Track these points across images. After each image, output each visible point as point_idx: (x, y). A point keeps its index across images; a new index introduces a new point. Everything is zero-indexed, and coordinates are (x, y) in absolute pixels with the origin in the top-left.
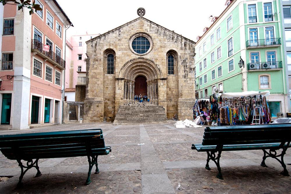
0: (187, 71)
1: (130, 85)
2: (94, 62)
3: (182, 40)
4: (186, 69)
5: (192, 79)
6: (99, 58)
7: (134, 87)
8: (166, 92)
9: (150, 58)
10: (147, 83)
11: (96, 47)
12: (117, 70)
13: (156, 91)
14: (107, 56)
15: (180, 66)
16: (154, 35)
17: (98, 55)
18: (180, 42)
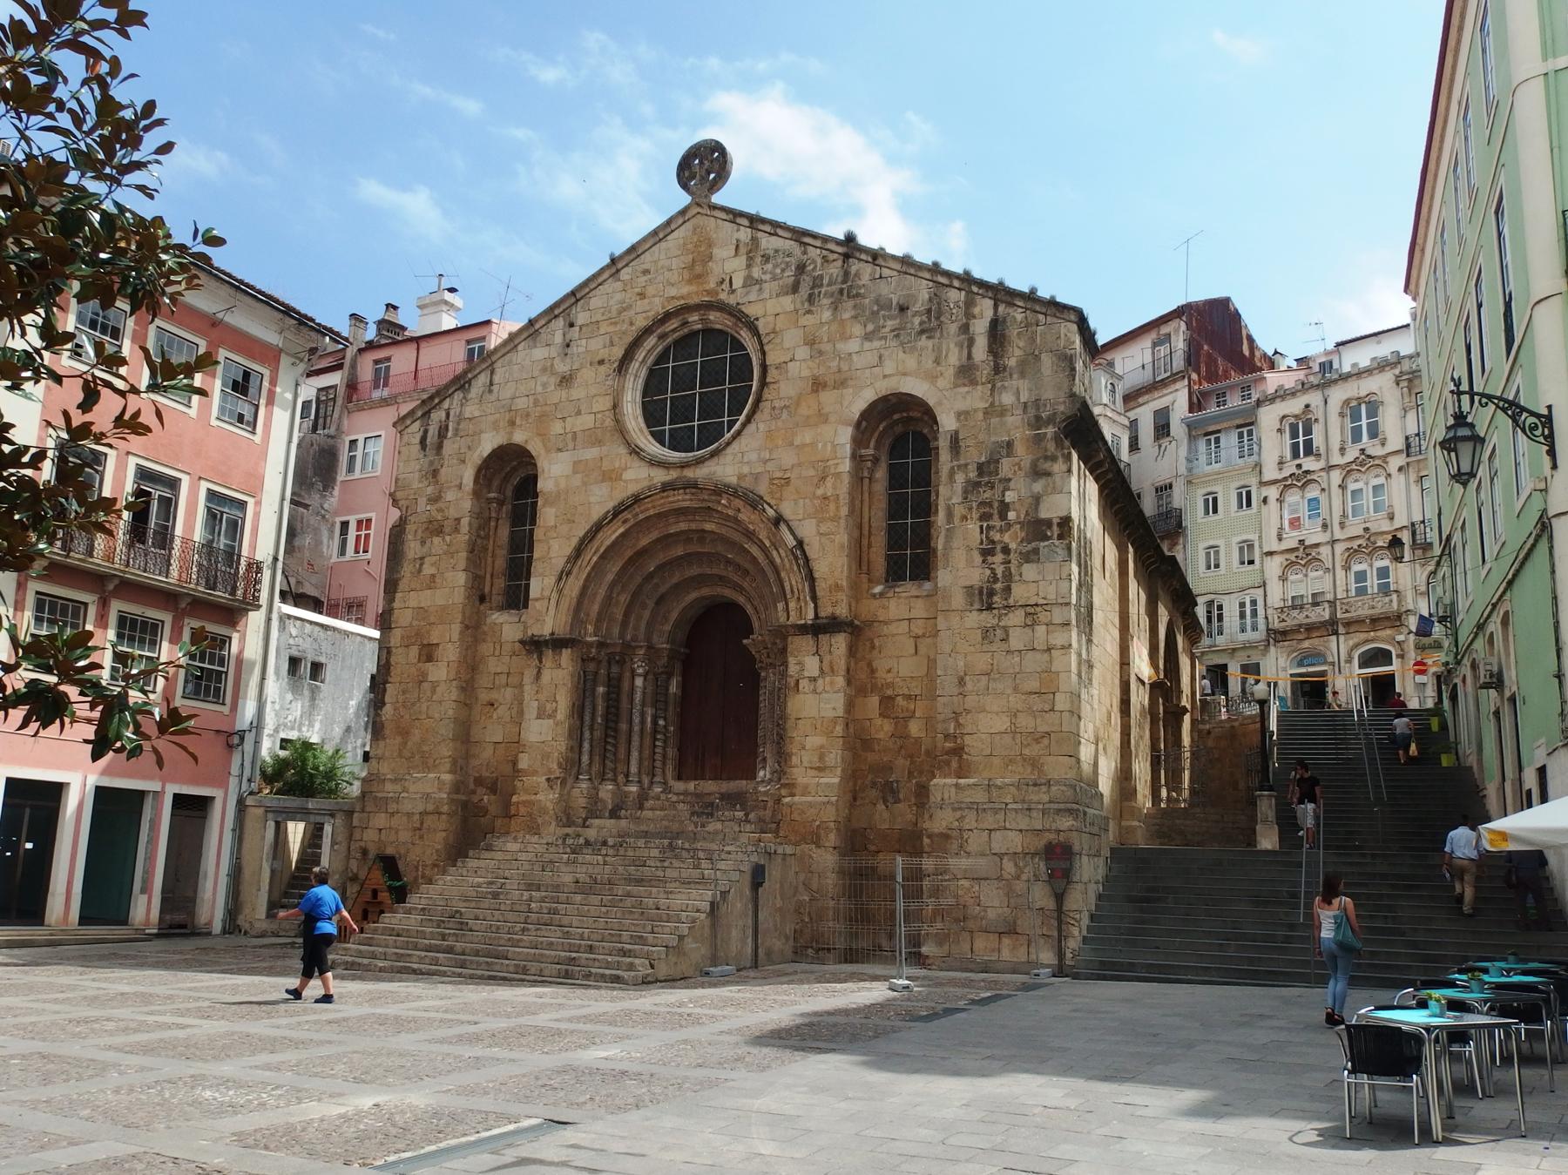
0: (1006, 550)
1: (639, 682)
2: (423, 543)
3: (976, 310)
4: (997, 537)
6: (452, 513)
7: (673, 688)
8: (839, 730)
9: (741, 477)
11: (439, 447)
12: (538, 585)
14: (509, 493)
16: (773, 306)
17: (450, 496)
18: (953, 328)
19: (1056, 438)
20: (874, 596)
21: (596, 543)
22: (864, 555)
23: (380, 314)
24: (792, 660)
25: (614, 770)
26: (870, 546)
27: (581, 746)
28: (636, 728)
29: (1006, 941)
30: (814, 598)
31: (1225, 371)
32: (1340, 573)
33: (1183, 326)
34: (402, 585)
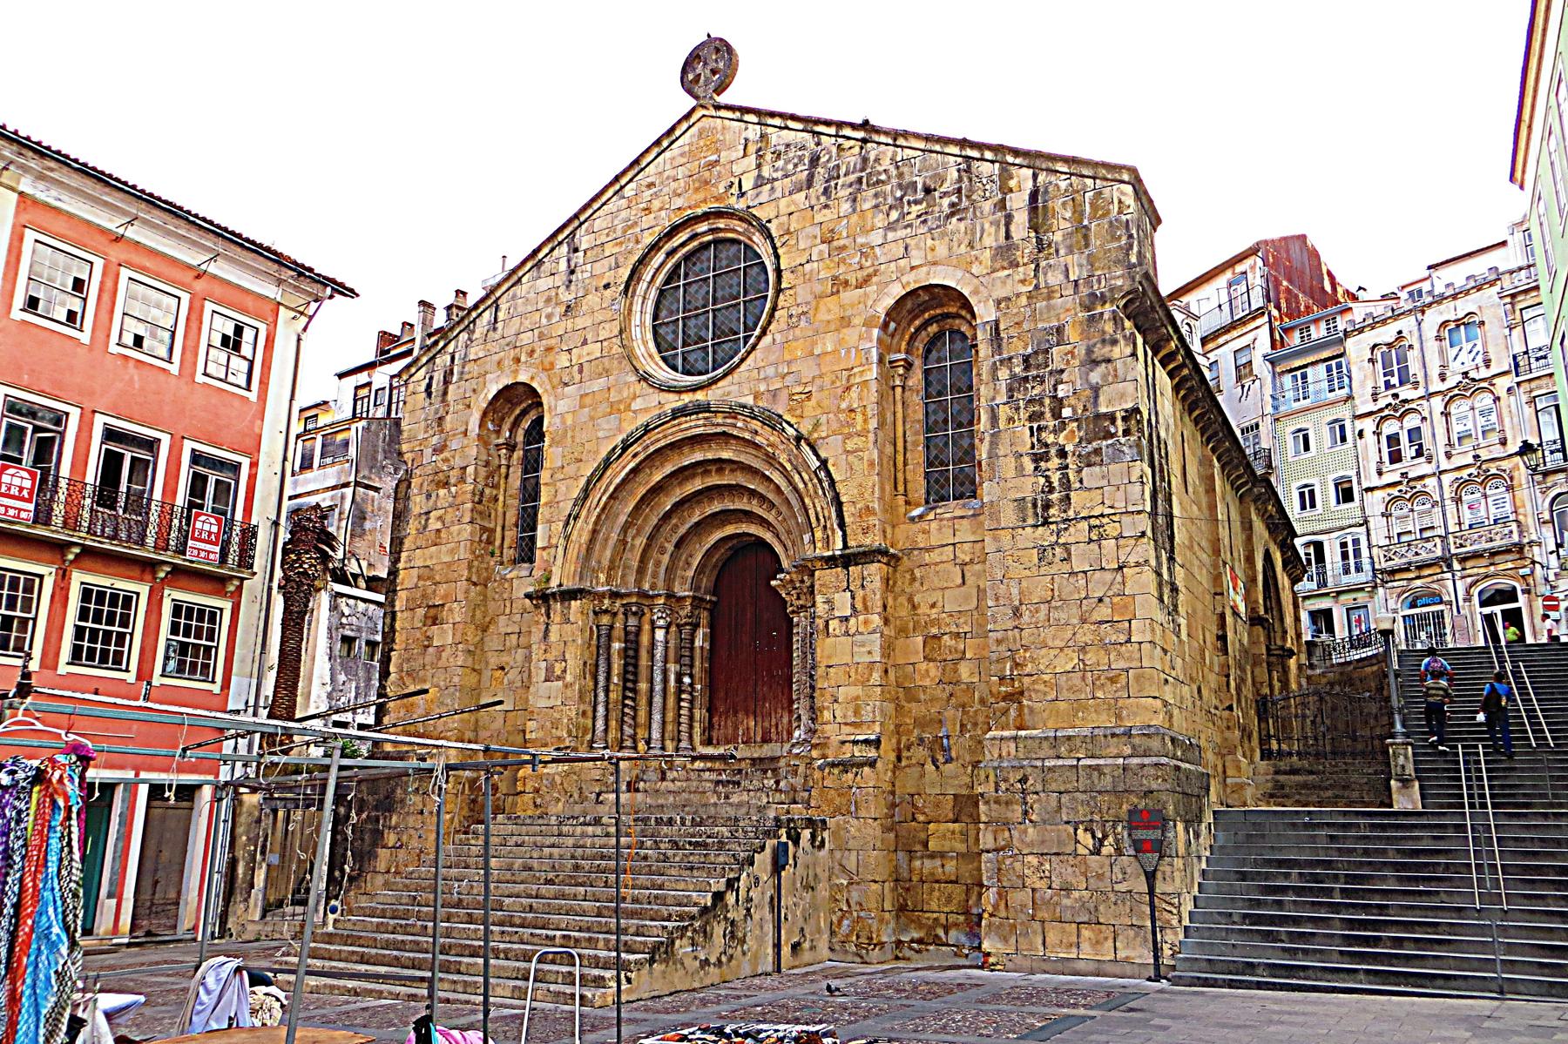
0: (1062, 454)
2: (429, 496)
4: (1050, 439)
5: (1112, 530)
6: (458, 462)
8: (876, 677)
11: (445, 393)
14: (520, 437)
15: (994, 419)
17: (454, 445)
18: (987, 206)
19: (1114, 317)
20: (912, 519)
21: (605, 480)
22: (900, 476)
23: (450, 299)
24: (819, 599)
25: (634, 737)
26: (905, 464)
27: (595, 710)
28: (658, 687)
29: (1086, 933)
30: (842, 525)
31: (1307, 307)
32: (1450, 507)
33: (1260, 263)
34: (407, 543)
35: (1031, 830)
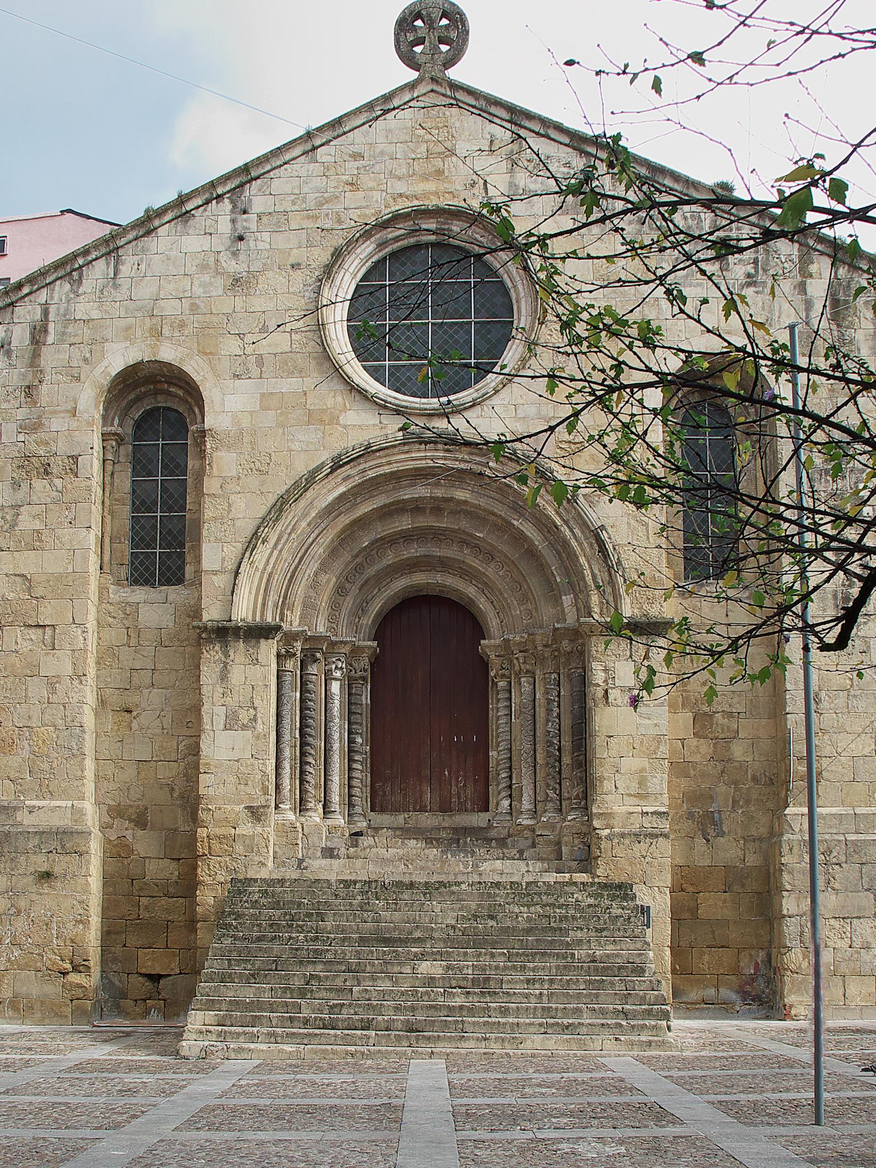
2: (16, 485)
6: (62, 447)
10: (484, 665)
11: (36, 355)
12: (214, 553)
13: (566, 743)
17: (56, 424)
35: (833, 897)
